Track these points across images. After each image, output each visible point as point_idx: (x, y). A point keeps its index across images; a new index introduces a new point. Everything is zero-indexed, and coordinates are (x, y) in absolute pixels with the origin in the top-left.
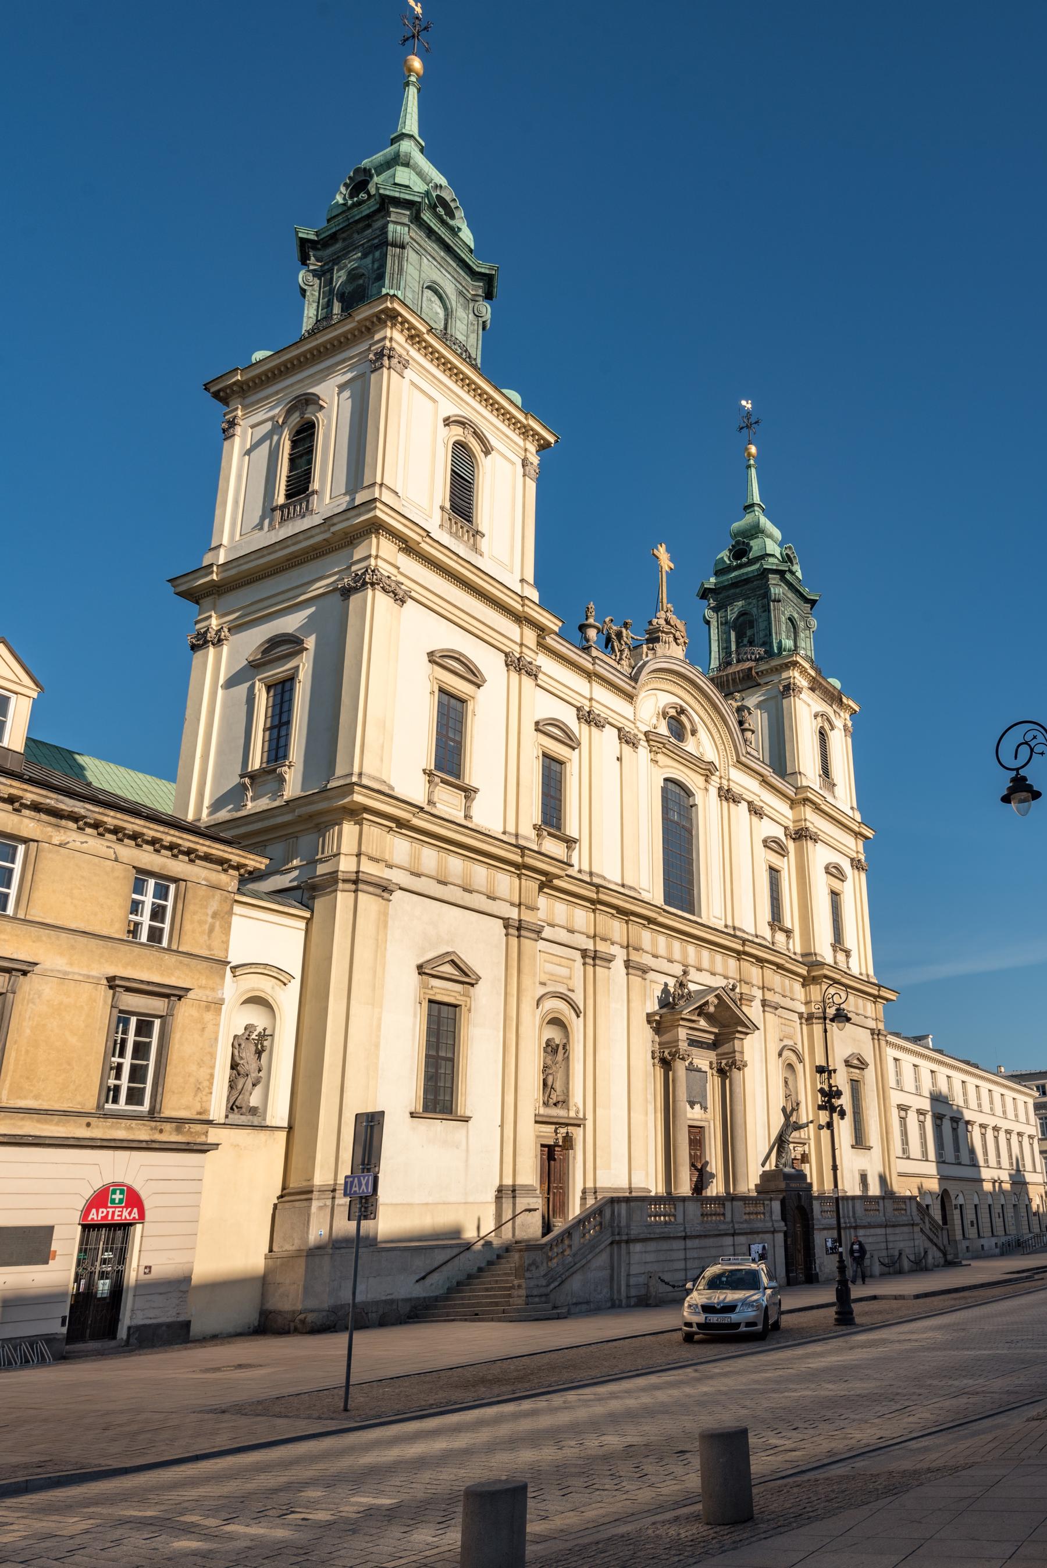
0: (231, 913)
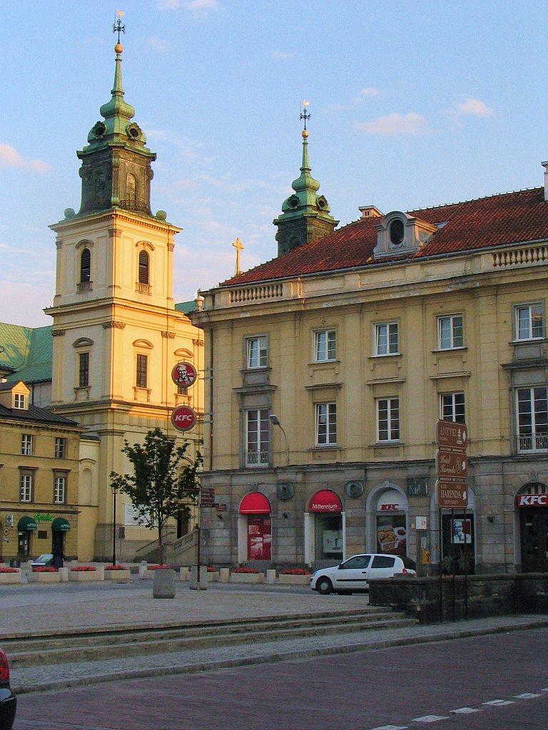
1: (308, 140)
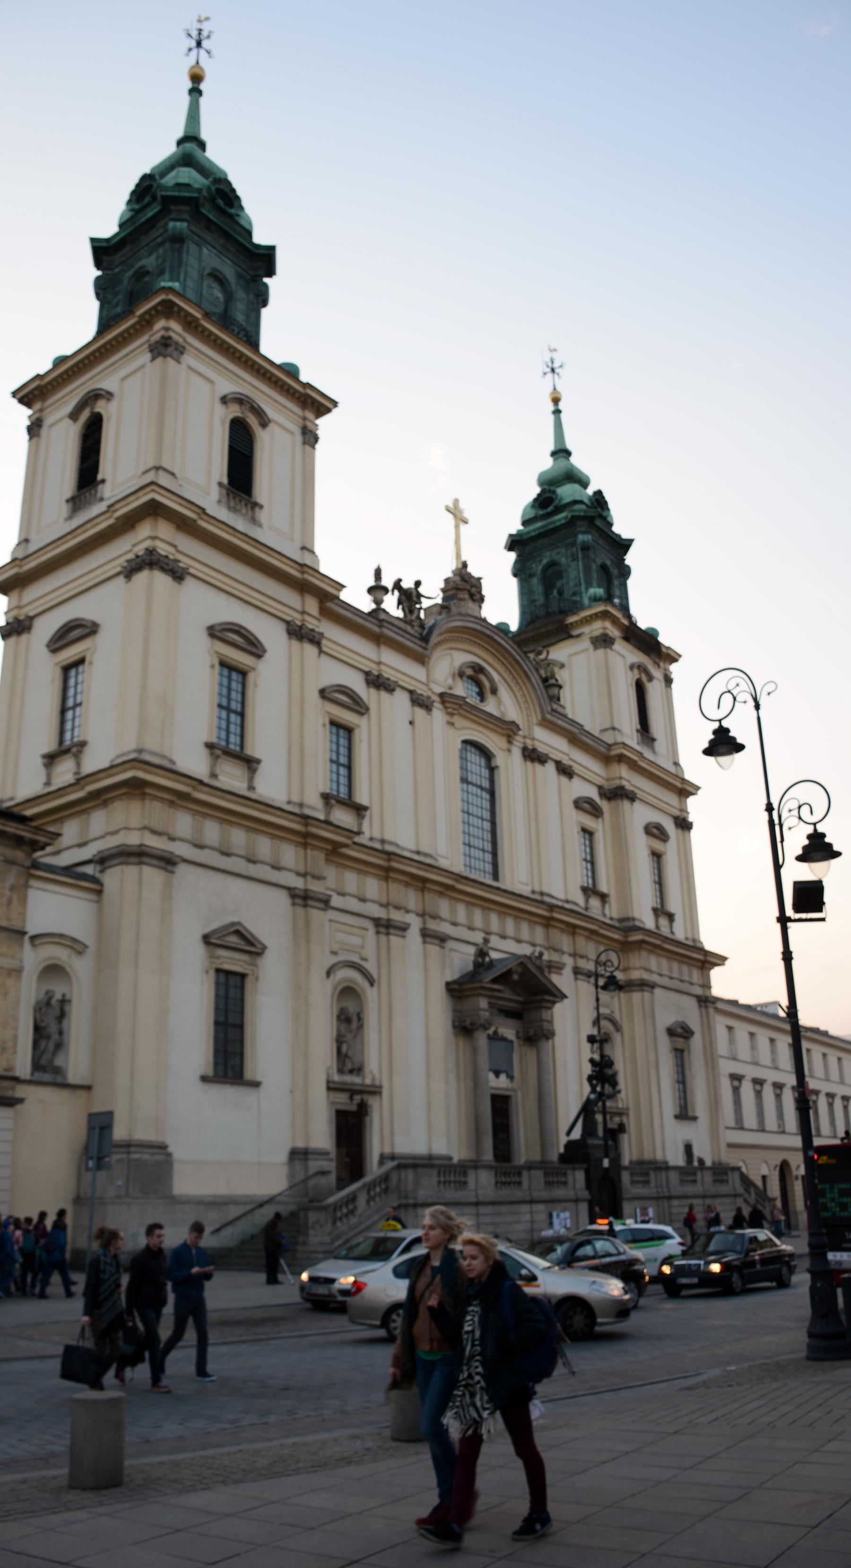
0: (27, 886)
1: (561, 406)
